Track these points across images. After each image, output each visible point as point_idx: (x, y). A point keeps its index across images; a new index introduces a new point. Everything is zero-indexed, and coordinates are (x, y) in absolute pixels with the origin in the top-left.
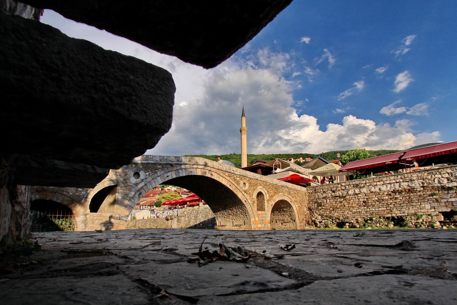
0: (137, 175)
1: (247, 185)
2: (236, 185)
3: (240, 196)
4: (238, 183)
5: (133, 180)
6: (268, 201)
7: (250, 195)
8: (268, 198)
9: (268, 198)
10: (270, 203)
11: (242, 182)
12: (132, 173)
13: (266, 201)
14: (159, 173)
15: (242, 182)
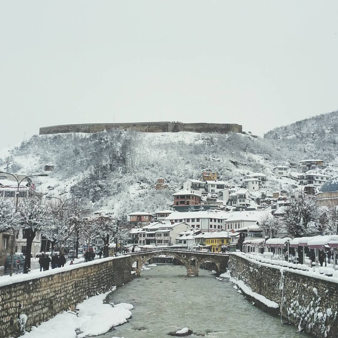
0: (143, 257)
1: (185, 256)
2: (179, 257)
3: (181, 261)
4: (181, 256)
5: (142, 259)
6: (197, 262)
7: (187, 260)
8: (197, 261)
9: (197, 261)
10: (199, 263)
11: (182, 256)
12: (141, 257)
13: (196, 262)
14: (149, 256)
15: (182, 256)
